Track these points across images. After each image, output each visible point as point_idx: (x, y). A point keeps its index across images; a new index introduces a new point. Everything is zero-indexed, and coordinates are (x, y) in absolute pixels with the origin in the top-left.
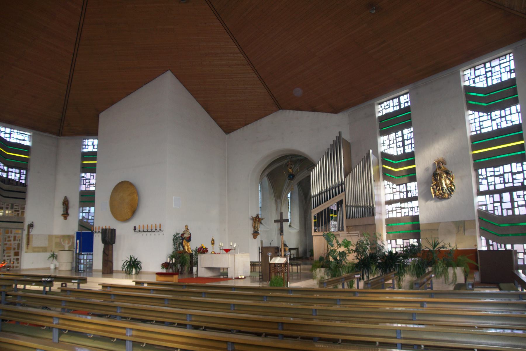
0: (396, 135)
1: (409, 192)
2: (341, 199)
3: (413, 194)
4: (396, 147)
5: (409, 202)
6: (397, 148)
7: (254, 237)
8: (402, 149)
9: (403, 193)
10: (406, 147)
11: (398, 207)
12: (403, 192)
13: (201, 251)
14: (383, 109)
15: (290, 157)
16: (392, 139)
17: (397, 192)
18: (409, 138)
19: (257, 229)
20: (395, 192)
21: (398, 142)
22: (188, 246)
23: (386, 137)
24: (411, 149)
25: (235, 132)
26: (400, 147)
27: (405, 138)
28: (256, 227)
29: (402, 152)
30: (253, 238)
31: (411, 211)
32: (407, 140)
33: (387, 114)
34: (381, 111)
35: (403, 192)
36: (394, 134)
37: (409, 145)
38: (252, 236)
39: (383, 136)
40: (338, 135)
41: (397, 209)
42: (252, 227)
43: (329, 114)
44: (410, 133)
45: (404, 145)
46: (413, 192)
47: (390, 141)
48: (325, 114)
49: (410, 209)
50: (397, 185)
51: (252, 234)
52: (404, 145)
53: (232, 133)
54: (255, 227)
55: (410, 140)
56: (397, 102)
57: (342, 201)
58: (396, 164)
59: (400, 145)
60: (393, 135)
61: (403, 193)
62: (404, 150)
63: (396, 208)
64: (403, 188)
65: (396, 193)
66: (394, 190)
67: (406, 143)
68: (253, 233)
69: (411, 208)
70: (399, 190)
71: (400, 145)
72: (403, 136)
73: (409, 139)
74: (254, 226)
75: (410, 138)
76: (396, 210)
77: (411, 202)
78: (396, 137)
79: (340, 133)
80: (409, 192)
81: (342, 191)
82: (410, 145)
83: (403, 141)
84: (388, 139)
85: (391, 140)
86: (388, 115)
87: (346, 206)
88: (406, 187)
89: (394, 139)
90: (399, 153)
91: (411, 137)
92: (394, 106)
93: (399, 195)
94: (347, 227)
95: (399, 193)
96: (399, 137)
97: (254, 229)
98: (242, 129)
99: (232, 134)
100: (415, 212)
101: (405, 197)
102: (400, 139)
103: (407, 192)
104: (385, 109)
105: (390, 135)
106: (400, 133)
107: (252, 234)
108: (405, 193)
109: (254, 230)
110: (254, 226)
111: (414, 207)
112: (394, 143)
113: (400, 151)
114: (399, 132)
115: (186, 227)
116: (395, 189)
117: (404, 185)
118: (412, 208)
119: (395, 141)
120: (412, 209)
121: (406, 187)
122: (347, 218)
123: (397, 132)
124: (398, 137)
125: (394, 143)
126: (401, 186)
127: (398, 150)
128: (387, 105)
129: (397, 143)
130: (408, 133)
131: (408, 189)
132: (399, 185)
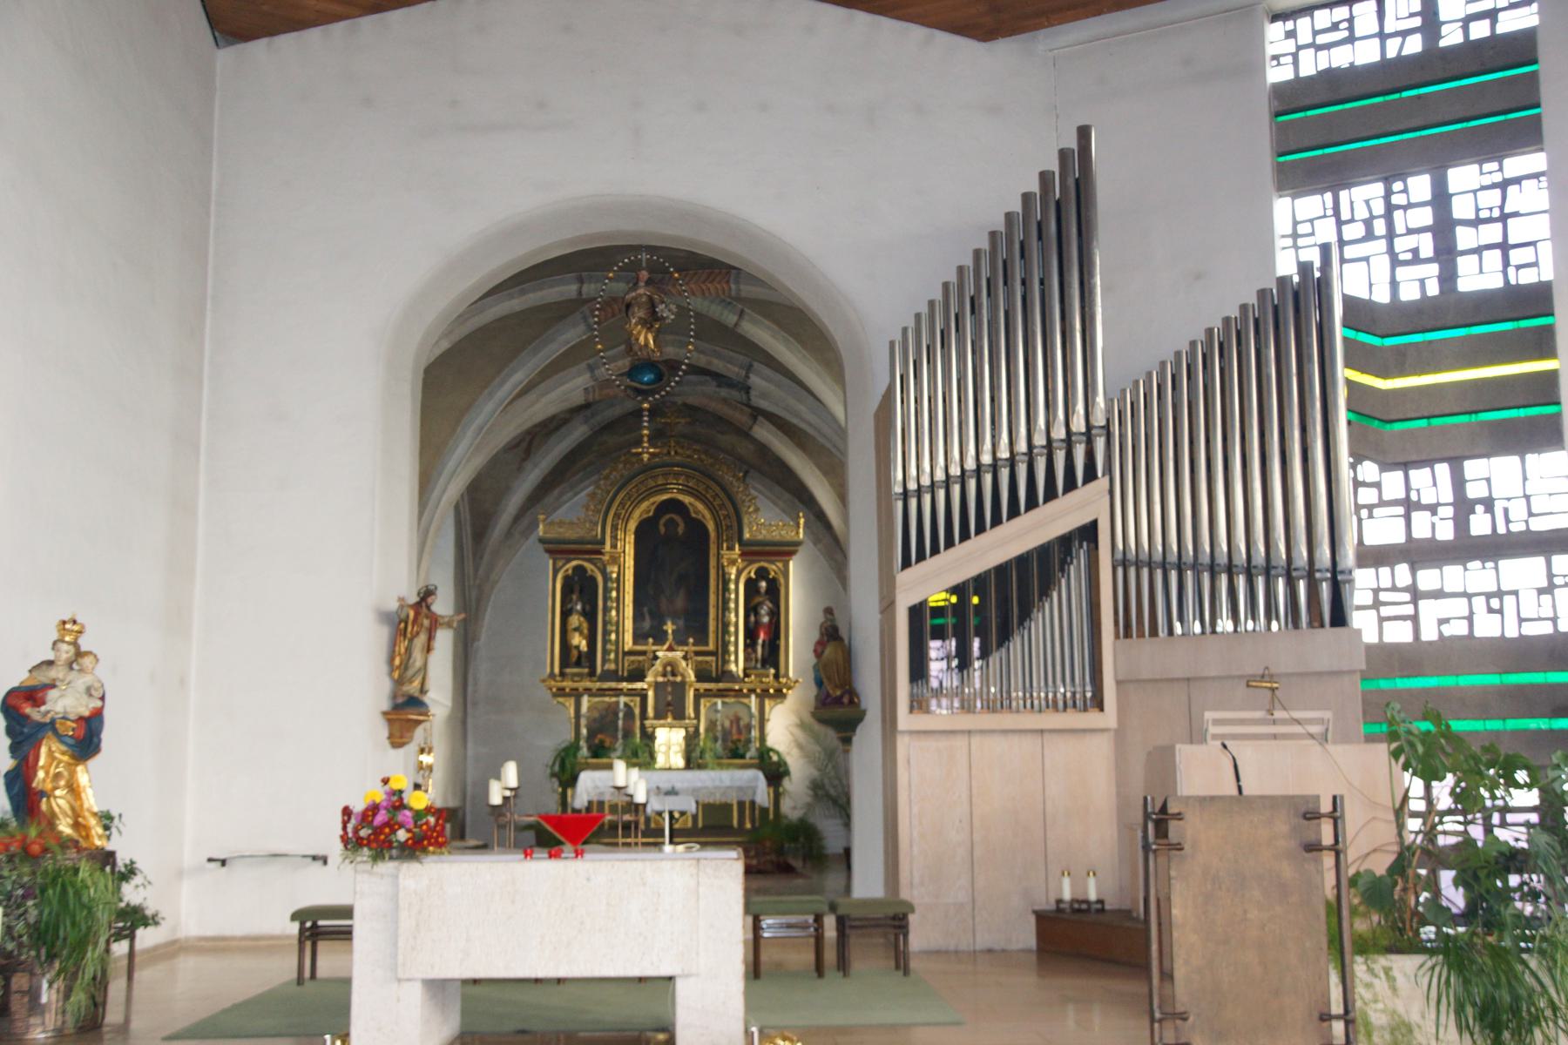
0: (1388, 194)
1: (1479, 508)
2: (1087, 519)
3: (1508, 521)
4: (1386, 259)
5: (1475, 565)
6: (1395, 262)
7: (391, 737)
8: (1434, 269)
9: (1434, 513)
10: (1465, 265)
11: (1394, 589)
12: (1433, 509)
13: (402, 835)
14: (1299, 48)
15: (644, 257)
16: (1362, 213)
17: (1383, 503)
18: (1484, 214)
19: (416, 684)
20: (1370, 507)
21: (1400, 228)
22: (74, 790)
23: (1312, 205)
24: (1501, 276)
25: (286, 41)
26: (1416, 259)
27: (1461, 208)
28: (410, 673)
29: (1433, 289)
30: (387, 743)
31: (1491, 610)
32: (1476, 222)
33: (1330, 77)
34: (1289, 59)
35: (1433, 509)
36: (1378, 189)
37: (1486, 254)
38: (383, 731)
39: (1294, 197)
40: (1072, 143)
41: (1383, 596)
42: (384, 668)
43: (943, 39)
44: (1493, 186)
45: (1446, 253)
46: (1506, 511)
47: (1340, 223)
48: (917, 32)
49: (1479, 603)
50: (1385, 467)
51: (385, 714)
52: (1446, 253)
53: (263, 42)
54: (405, 666)
55: (1499, 225)
56: (1412, 15)
57: (1089, 532)
58: (1382, 349)
59: (1415, 251)
60: (1365, 196)
61: (1434, 513)
62: (1448, 277)
63: (1376, 591)
64: (1432, 483)
65: (1376, 512)
66: (1367, 496)
67: (1465, 238)
68: (386, 705)
69: (1489, 596)
70: (1402, 495)
71: (1415, 251)
72: (1441, 199)
73: (1490, 220)
74: (397, 662)
75: (1496, 213)
76: (1377, 604)
77: (1490, 565)
78: (1390, 208)
79: (1084, 133)
80: (1479, 508)
81: (1090, 475)
82: (1497, 253)
83: (1444, 228)
84: (1330, 212)
85: (1352, 220)
86: (1335, 85)
87: (1122, 563)
88: (1459, 482)
89: (1372, 217)
90: (1409, 293)
91: (1502, 208)
92: (1382, 36)
93: (1402, 521)
94: (1119, 683)
95: (1400, 510)
96: (1410, 206)
97: (399, 683)
98: (338, 28)
99: (258, 49)
100: (1521, 620)
101: (1446, 532)
102: (1425, 217)
103: (1463, 507)
104: (1319, 48)
105: (1344, 195)
106: (1420, 186)
107: (385, 714)
108: (1448, 512)
109: (394, 696)
110: (397, 662)
111: (1515, 593)
112: (1369, 236)
113: (1419, 283)
114: (1411, 181)
115: (69, 629)
116: (1374, 491)
117: (1443, 470)
118: (1500, 594)
119: (1380, 227)
120: (1495, 603)
121: (1459, 482)
122: (1125, 630)
123: (1403, 177)
124: (1404, 202)
125: (1369, 236)
126: (1419, 477)
127: (1398, 278)
128: (1335, 27)
129: (1397, 241)
130: (1483, 188)
131: (1474, 491)
132: (1406, 466)
